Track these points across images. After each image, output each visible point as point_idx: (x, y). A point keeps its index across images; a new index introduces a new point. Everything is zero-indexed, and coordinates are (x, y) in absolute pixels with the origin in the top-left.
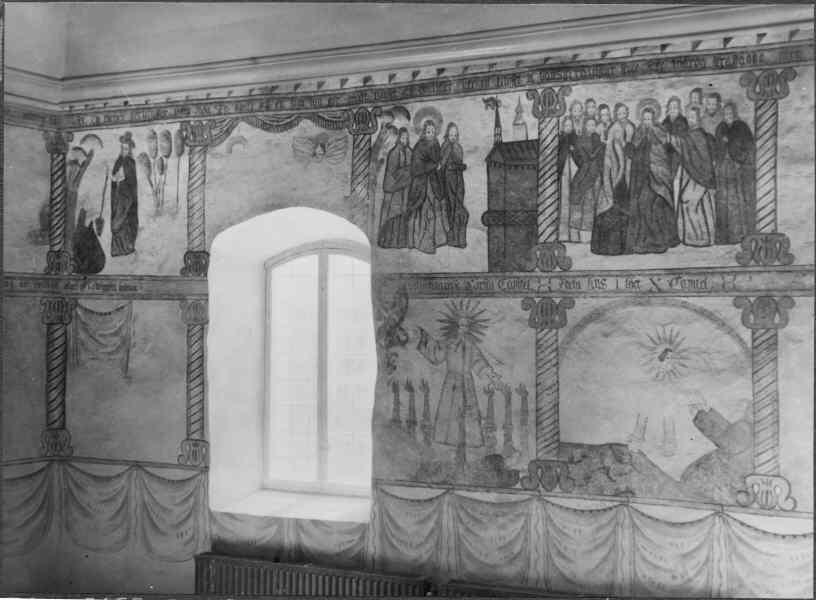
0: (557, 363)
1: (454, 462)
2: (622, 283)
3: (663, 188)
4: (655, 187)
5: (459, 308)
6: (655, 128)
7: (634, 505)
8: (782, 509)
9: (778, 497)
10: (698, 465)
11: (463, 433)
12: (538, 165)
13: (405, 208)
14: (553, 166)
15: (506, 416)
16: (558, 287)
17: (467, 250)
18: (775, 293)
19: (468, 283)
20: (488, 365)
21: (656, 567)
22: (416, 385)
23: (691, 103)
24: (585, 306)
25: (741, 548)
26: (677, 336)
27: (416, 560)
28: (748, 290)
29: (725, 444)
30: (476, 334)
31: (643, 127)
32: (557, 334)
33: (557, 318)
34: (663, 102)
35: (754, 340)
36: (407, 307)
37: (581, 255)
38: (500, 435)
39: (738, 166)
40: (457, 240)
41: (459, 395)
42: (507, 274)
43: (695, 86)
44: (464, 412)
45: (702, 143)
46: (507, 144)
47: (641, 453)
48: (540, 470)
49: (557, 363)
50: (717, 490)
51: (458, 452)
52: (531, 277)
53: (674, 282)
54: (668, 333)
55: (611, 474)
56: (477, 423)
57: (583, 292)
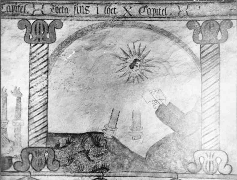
0: (47, 71)
9: (218, 165)
16: (50, 11)
18: (218, 18)
24: (72, 27)
28: (197, 16)
29: (179, 129)
32: (48, 47)
33: (48, 36)
35: (202, 53)
47: (114, 138)
48: (31, 156)
49: (47, 71)
50: (173, 163)
53: (142, 10)
54: (137, 48)
55: (90, 156)
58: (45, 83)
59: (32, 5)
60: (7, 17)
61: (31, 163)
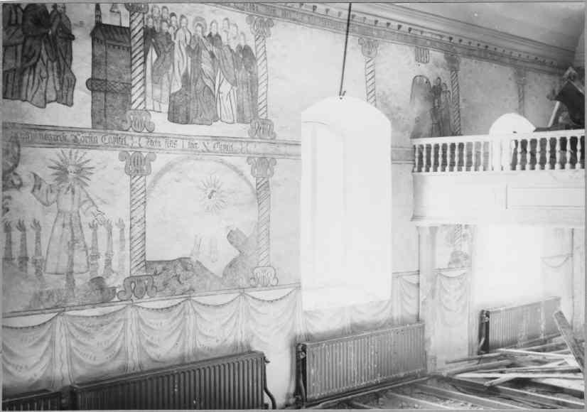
0: (145, 202)
1: (64, 288)
2: (186, 143)
3: (209, 81)
4: (205, 80)
5: (68, 156)
6: (203, 39)
7: (194, 298)
8: (272, 286)
10: (230, 265)
11: (72, 264)
12: (131, 48)
13: (19, 64)
14: (140, 52)
15: (108, 245)
17: (72, 108)
19: (76, 137)
20: (94, 204)
21: (207, 336)
22: (28, 224)
23: (223, 27)
25: (253, 313)
26: (218, 182)
27: (30, 380)
30: (84, 180)
31: (196, 36)
32: (145, 180)
33: (145, 168)
34: (208, 23)
35: (258, 184)
36: (19, 155)
37: (161, 122)
38: (101, 261)
39: (249, 75)
40: (65, 98)
41: (67, 230)
42: (109, 131)
43: (226, 17)
44: (73, 244)
45: (229, 56)
46: (105, 25)
48: (133, 284)
49: (145, 202)
51: (68, 279)
52: (127, 135)
53: (216, 146)
55: (181, 280)
56: (85, 252)
57: (163, 149)
58: (143, 213)
59: (130, 137)
60: (109, 148)
61: (133, 292)
